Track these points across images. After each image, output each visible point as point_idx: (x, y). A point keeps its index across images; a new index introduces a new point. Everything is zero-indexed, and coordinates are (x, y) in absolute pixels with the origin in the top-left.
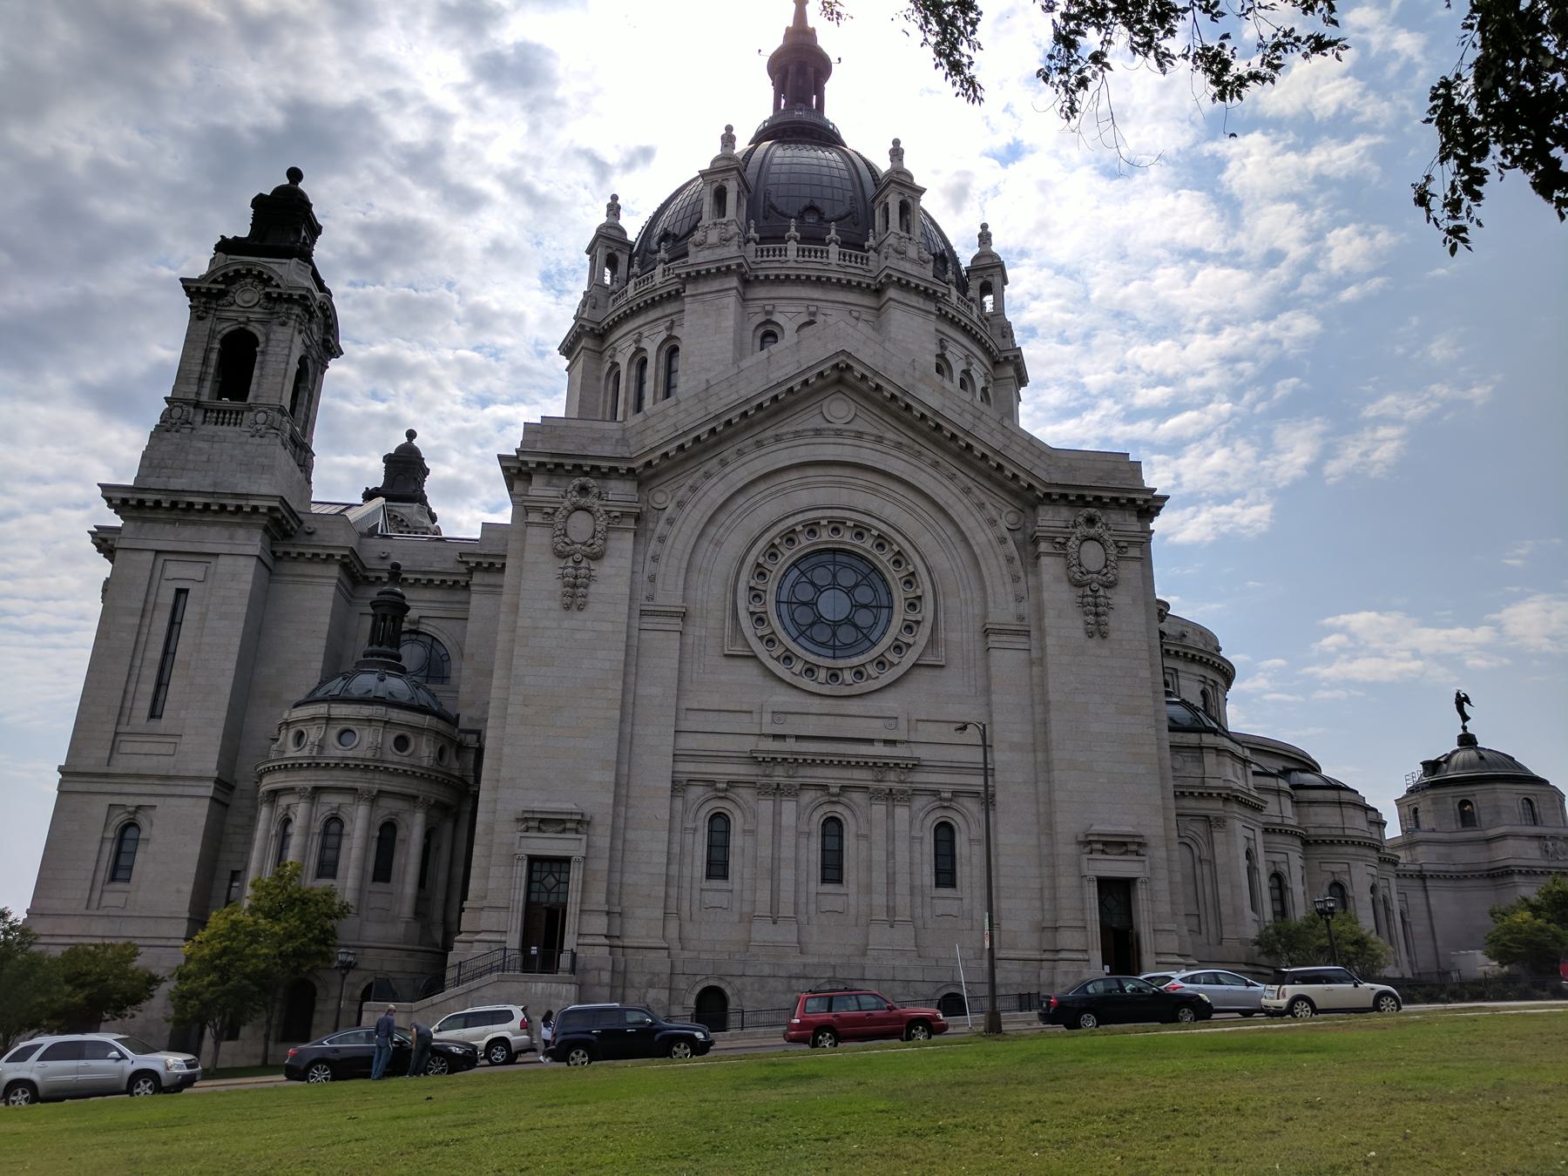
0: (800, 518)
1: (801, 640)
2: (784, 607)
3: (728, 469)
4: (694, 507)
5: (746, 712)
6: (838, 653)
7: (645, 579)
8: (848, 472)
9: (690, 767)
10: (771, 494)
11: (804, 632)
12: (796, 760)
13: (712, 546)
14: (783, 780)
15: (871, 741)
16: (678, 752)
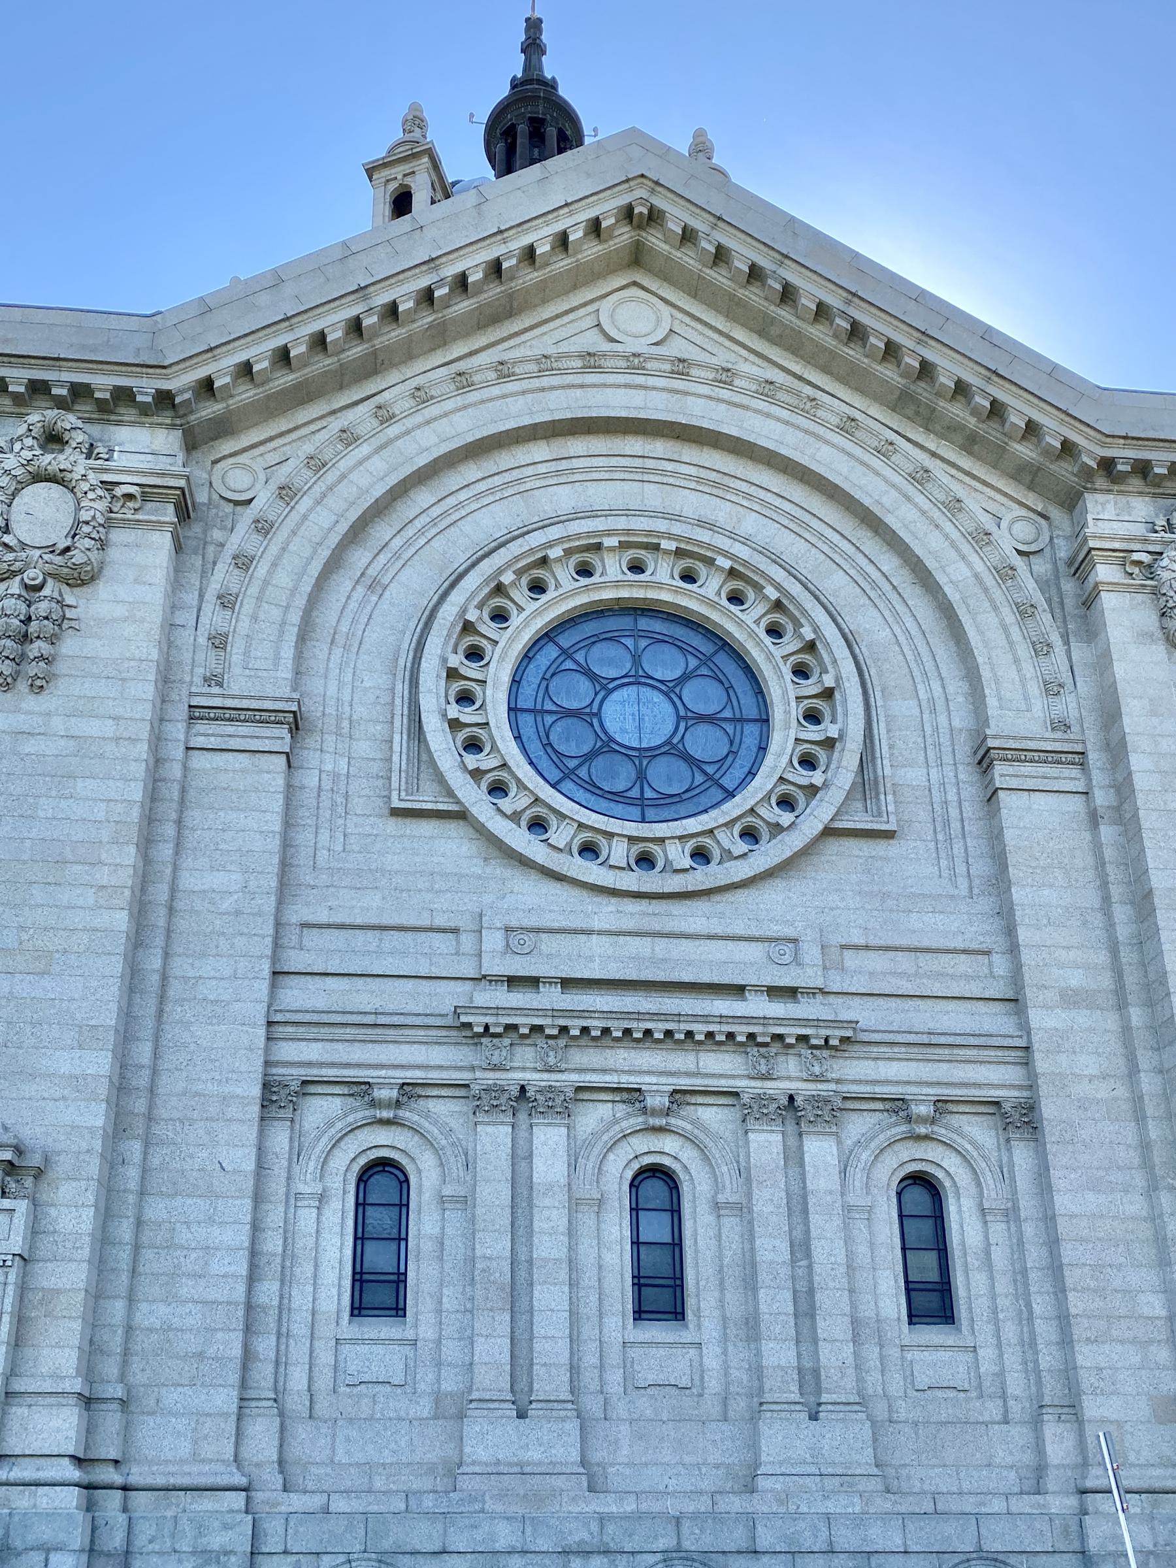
0: (554, 532)
1: (568, 786)
2: (526, 720)
3: (393, 430)
4: (318, 502)
5: (443, 930)
6: (650, 813)
7: (202, 641)
8: (659, 447)
9: (313, 1052)
10: (491, 490)
11: (573, 771)
12: (564, 1030)
13: (360, 590)
14: (536, 1079)
15: (739, 990)
16: (278, 1017)
